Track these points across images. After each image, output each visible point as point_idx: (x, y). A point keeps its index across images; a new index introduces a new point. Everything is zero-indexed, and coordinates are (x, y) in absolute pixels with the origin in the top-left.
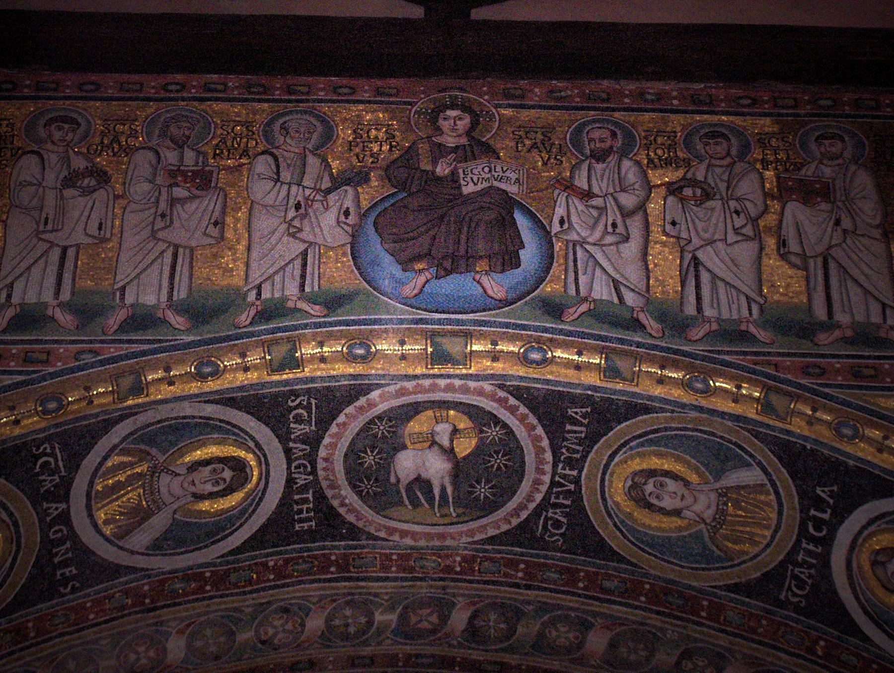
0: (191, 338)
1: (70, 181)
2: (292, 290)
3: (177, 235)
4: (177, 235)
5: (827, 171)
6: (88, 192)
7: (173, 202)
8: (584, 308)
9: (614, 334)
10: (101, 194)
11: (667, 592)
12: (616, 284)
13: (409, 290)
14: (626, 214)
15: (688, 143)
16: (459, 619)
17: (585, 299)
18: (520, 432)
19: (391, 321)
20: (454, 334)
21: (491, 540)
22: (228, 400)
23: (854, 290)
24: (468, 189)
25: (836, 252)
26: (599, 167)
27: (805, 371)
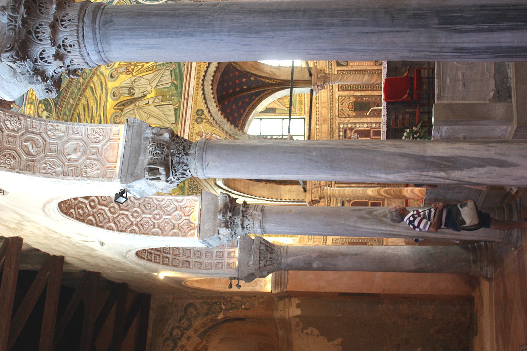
11: (68, 85)
13: (17, 107)
19: (24, 110)
20: (29, 100)
21: (55, 110)
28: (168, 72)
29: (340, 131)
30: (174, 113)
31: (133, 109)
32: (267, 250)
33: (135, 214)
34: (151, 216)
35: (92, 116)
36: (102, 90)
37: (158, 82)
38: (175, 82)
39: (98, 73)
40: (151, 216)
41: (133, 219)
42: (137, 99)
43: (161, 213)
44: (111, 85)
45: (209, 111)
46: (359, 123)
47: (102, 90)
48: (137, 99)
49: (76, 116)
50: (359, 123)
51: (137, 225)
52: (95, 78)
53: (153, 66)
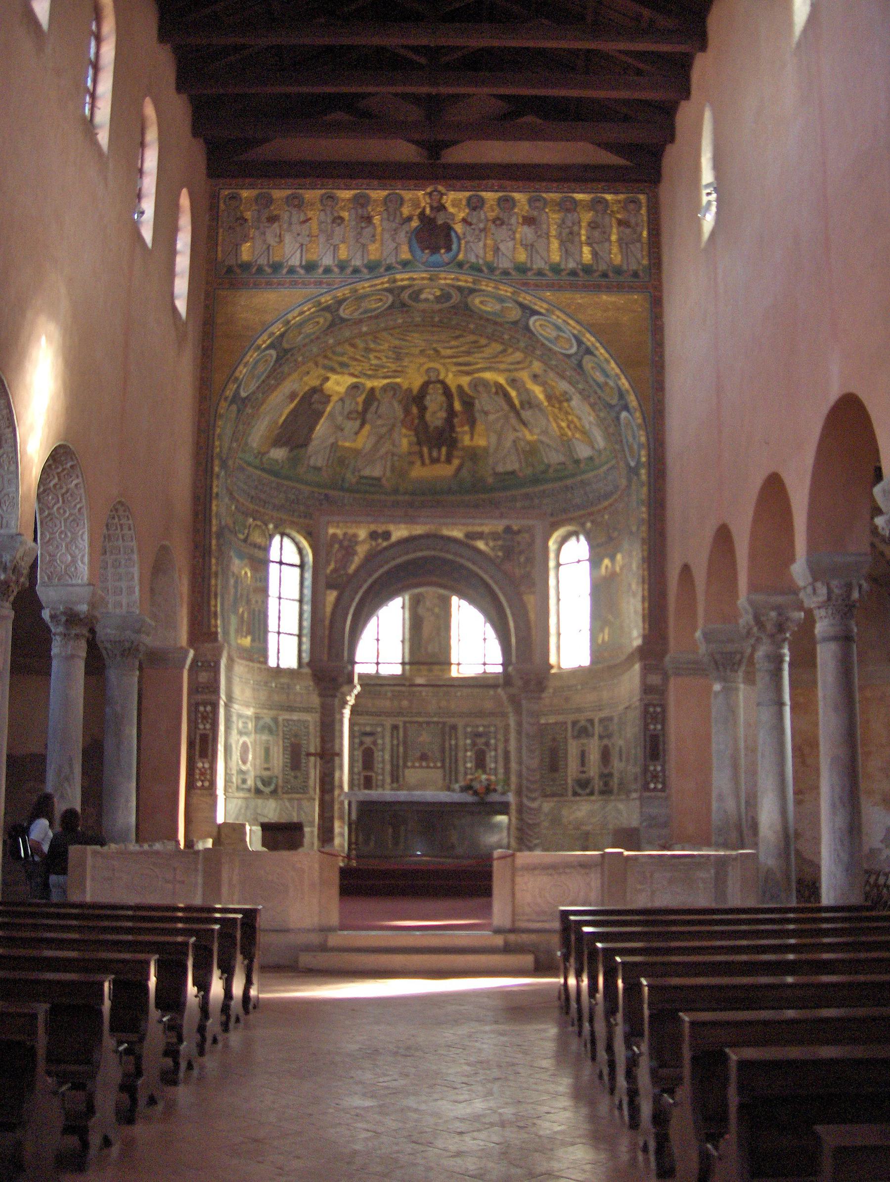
0: (368, 277)
1: (333, 222)
2: (394, 261)
3: (362, 241)
4: (362, 241)
5: (535, 213)
6: (339, 225)
7: (362, 228)
8: (468, 265)
9: (476, 273)
10: (342, 226)
12: (477, 256)
13: (424, 260)
14: (481, 231)
15: (499, 205)
16: (437, 319)
17: (468, 262)
18: (451, 291)
22: (379, 290)
23: (539, 257)
24: (440, 222)
25: (535, 244)
26: (475, 213)
27: (525, 284)
28: (562, 458)
29: (484, 726)
30: (509, 468)
31: (502, 410)
32: (125, 650)
33: (62, 511)
34: (63, 528)
35: (474, 353)
36: (512, 364)
37: (548, 446)
38: (551, 470)
39: (529, 359)
40: (63, 528)
41: (55, 509)
42: (518, 414)
43: (68, 540)
44: (524, 376)
45: (385, 549)
46: (496, 757)
47: (512, 364)
48: (518, 414)
49: (458, 333)
50: (496, 757)
51: (49, 514)
52: (518, 356)
53: (566, 435)
